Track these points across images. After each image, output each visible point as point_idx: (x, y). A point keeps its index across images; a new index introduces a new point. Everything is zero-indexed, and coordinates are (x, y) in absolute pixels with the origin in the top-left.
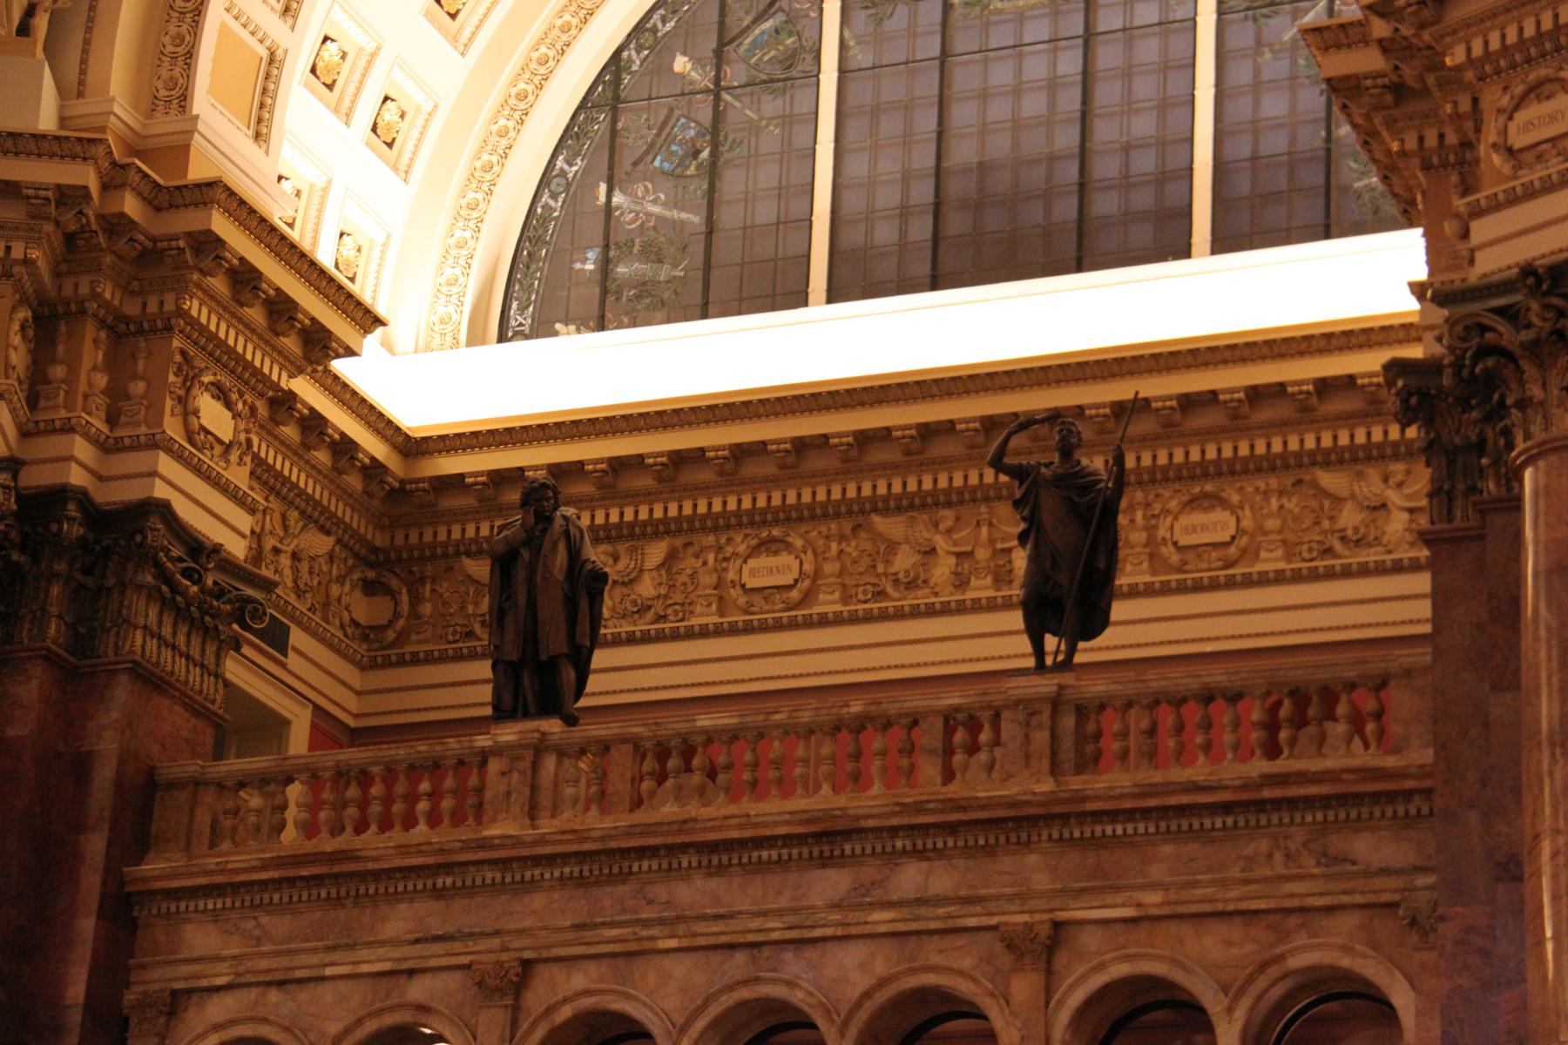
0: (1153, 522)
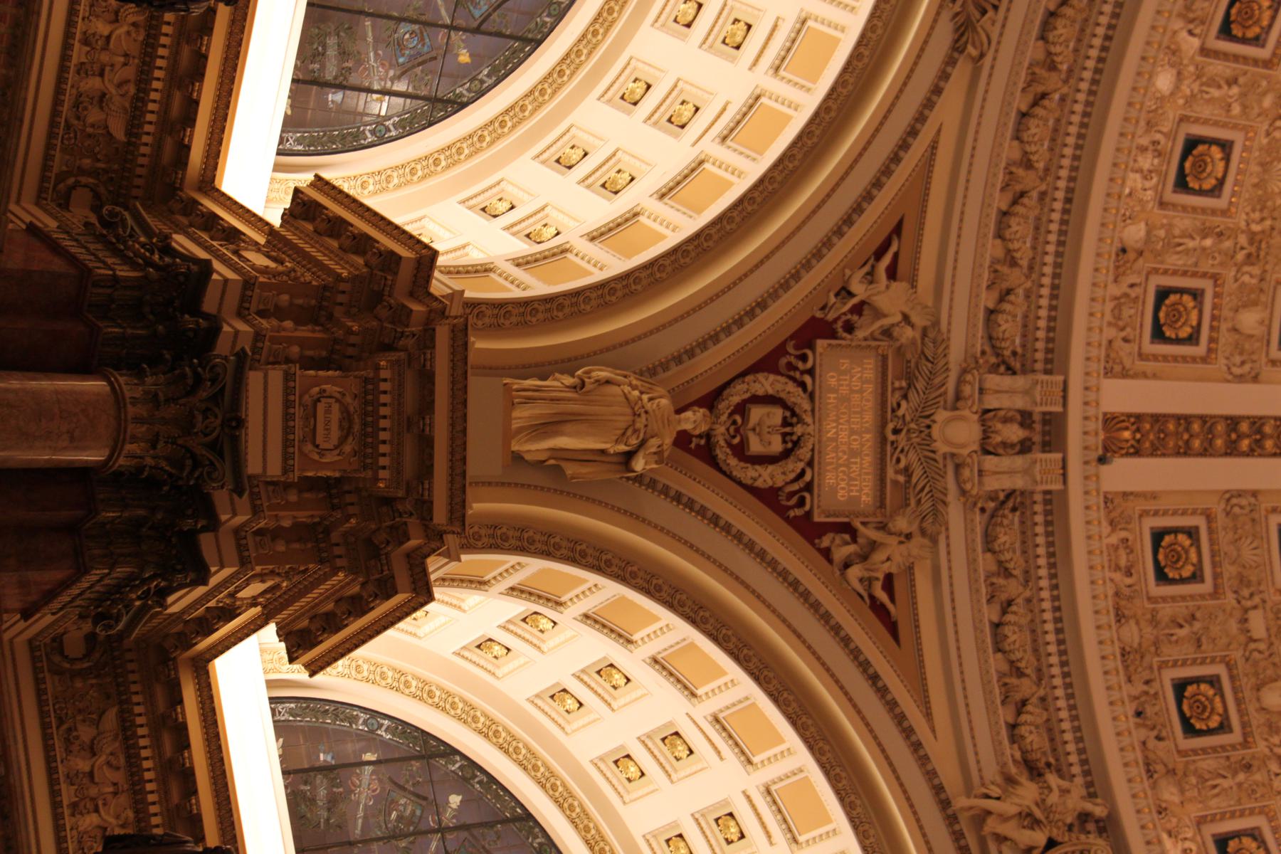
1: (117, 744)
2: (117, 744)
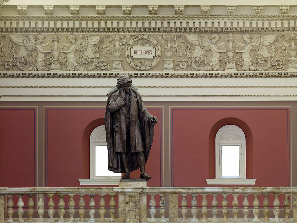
0: (123, 47)
1: (31, 36)
2: (31, 36)
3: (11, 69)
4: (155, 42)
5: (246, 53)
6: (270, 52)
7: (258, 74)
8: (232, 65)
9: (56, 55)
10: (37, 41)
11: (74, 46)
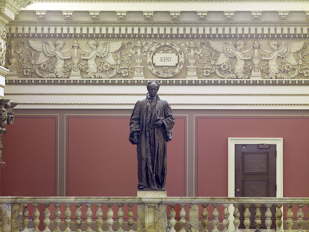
0: (145, 54)
1: (50, 42)
2: (50, 42)
3: (30, 75)
4: (178, 49)
5: (273, 60)
6: (297, 60)
7: (284, 82)
8: (257, 73)
9: (76, 61)
10: (57, 47)
11: (95, 52)
